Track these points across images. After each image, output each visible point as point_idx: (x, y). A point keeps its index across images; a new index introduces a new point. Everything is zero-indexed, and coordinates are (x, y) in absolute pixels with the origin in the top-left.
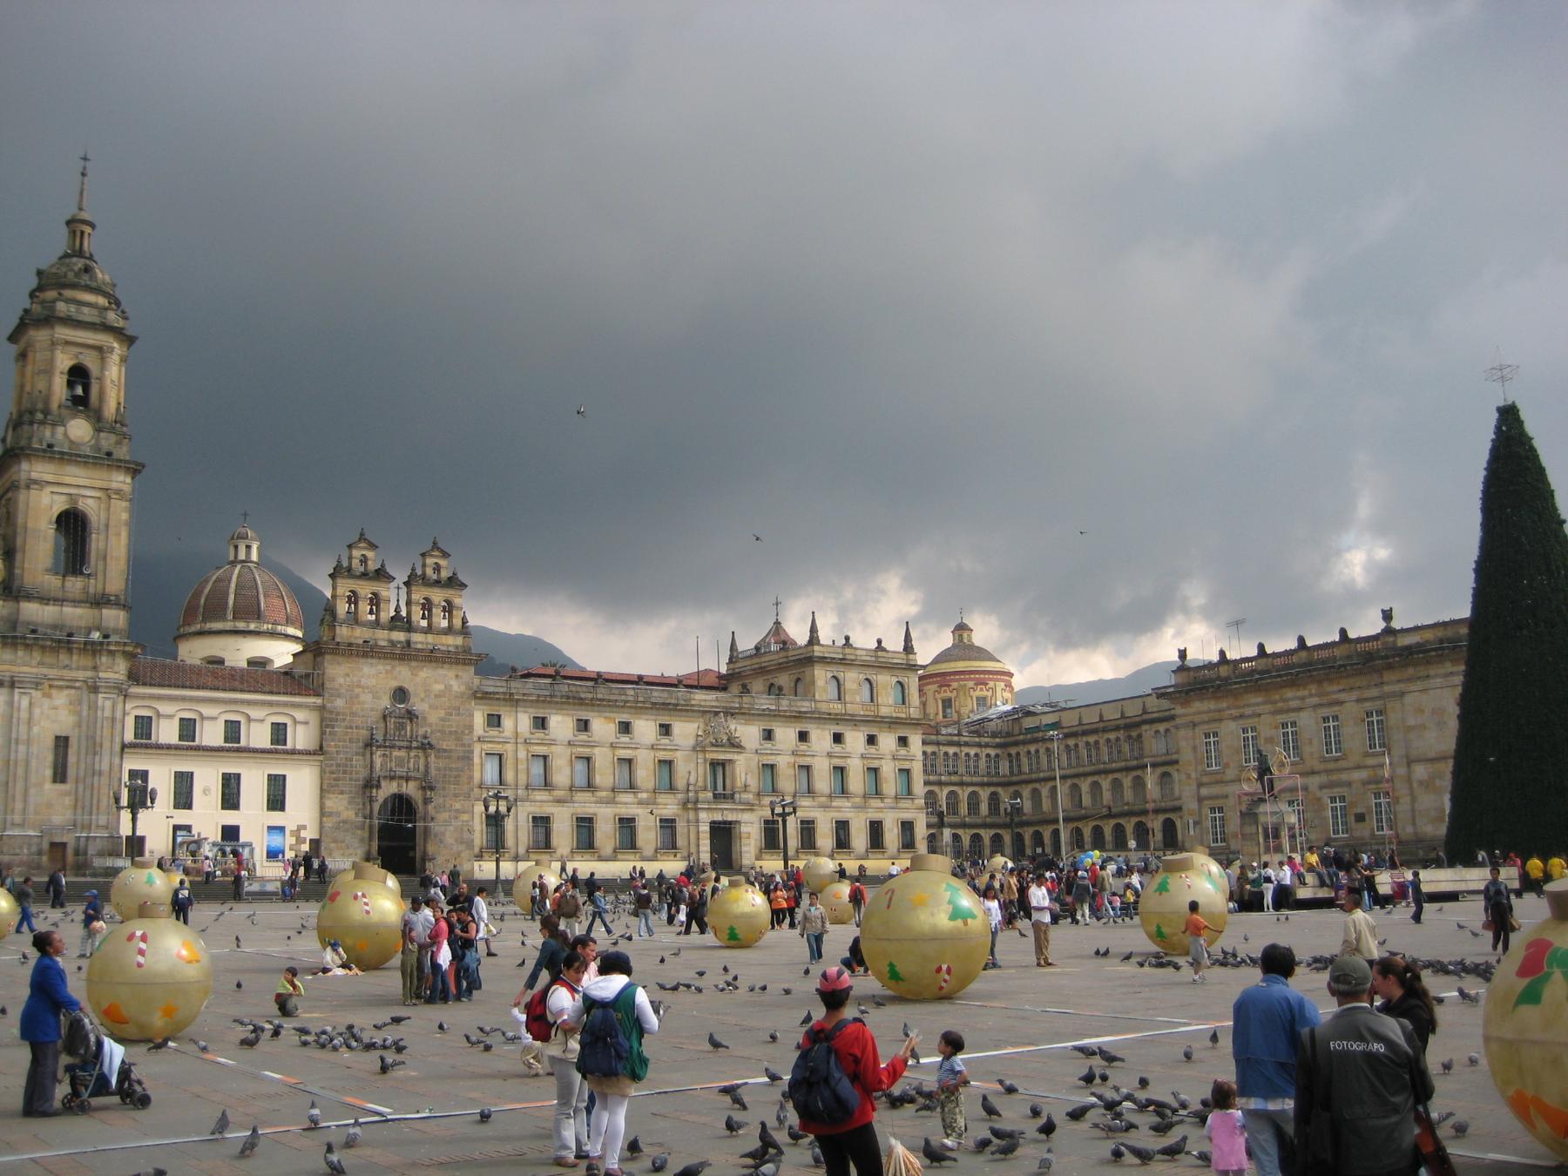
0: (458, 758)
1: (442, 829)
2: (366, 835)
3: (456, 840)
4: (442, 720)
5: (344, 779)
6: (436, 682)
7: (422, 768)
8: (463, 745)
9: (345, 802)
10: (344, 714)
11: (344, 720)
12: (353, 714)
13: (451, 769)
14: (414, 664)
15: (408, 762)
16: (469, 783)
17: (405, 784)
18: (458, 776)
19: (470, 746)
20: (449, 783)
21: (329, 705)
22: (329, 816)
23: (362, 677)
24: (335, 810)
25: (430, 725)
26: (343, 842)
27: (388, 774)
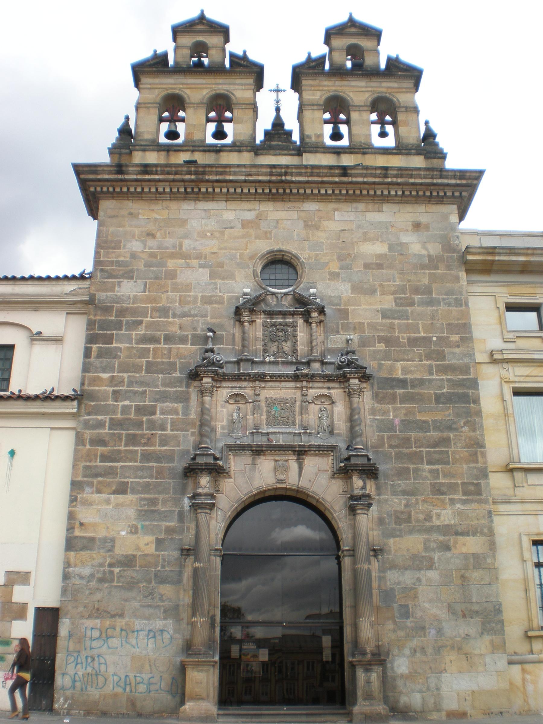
0: (438, 399)
1: (408, 578)
2: (186, 599)
3: (450, 607)
4: (385, 314)
5: (131, 456)
6: (366, 239)
7: (341, 426)
8: (451, 369)
9: (131, 512)
10: (134, 312)
11: (141, 322)
12: (164, 312)
13: (423, 426)
14: (311, 207)
15: (303, 410)
16: (474, 457)
17: (293, 465)
18: (446, 441)
19: (465, 369)
20: (416, 457)
21: (101, 295)
22: (84, 548)
23: (186, 237)
24: (102, 533)
25: (358, 327)
26: (122, 615)
27: (247, 441)
